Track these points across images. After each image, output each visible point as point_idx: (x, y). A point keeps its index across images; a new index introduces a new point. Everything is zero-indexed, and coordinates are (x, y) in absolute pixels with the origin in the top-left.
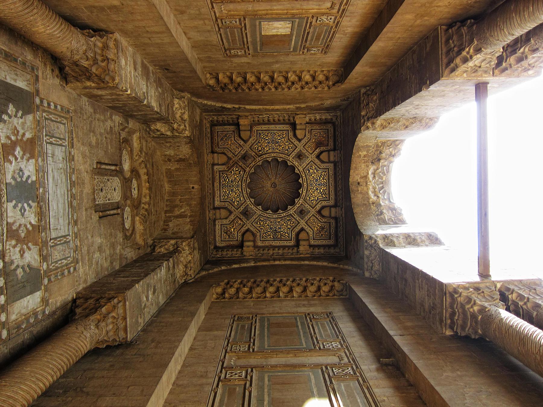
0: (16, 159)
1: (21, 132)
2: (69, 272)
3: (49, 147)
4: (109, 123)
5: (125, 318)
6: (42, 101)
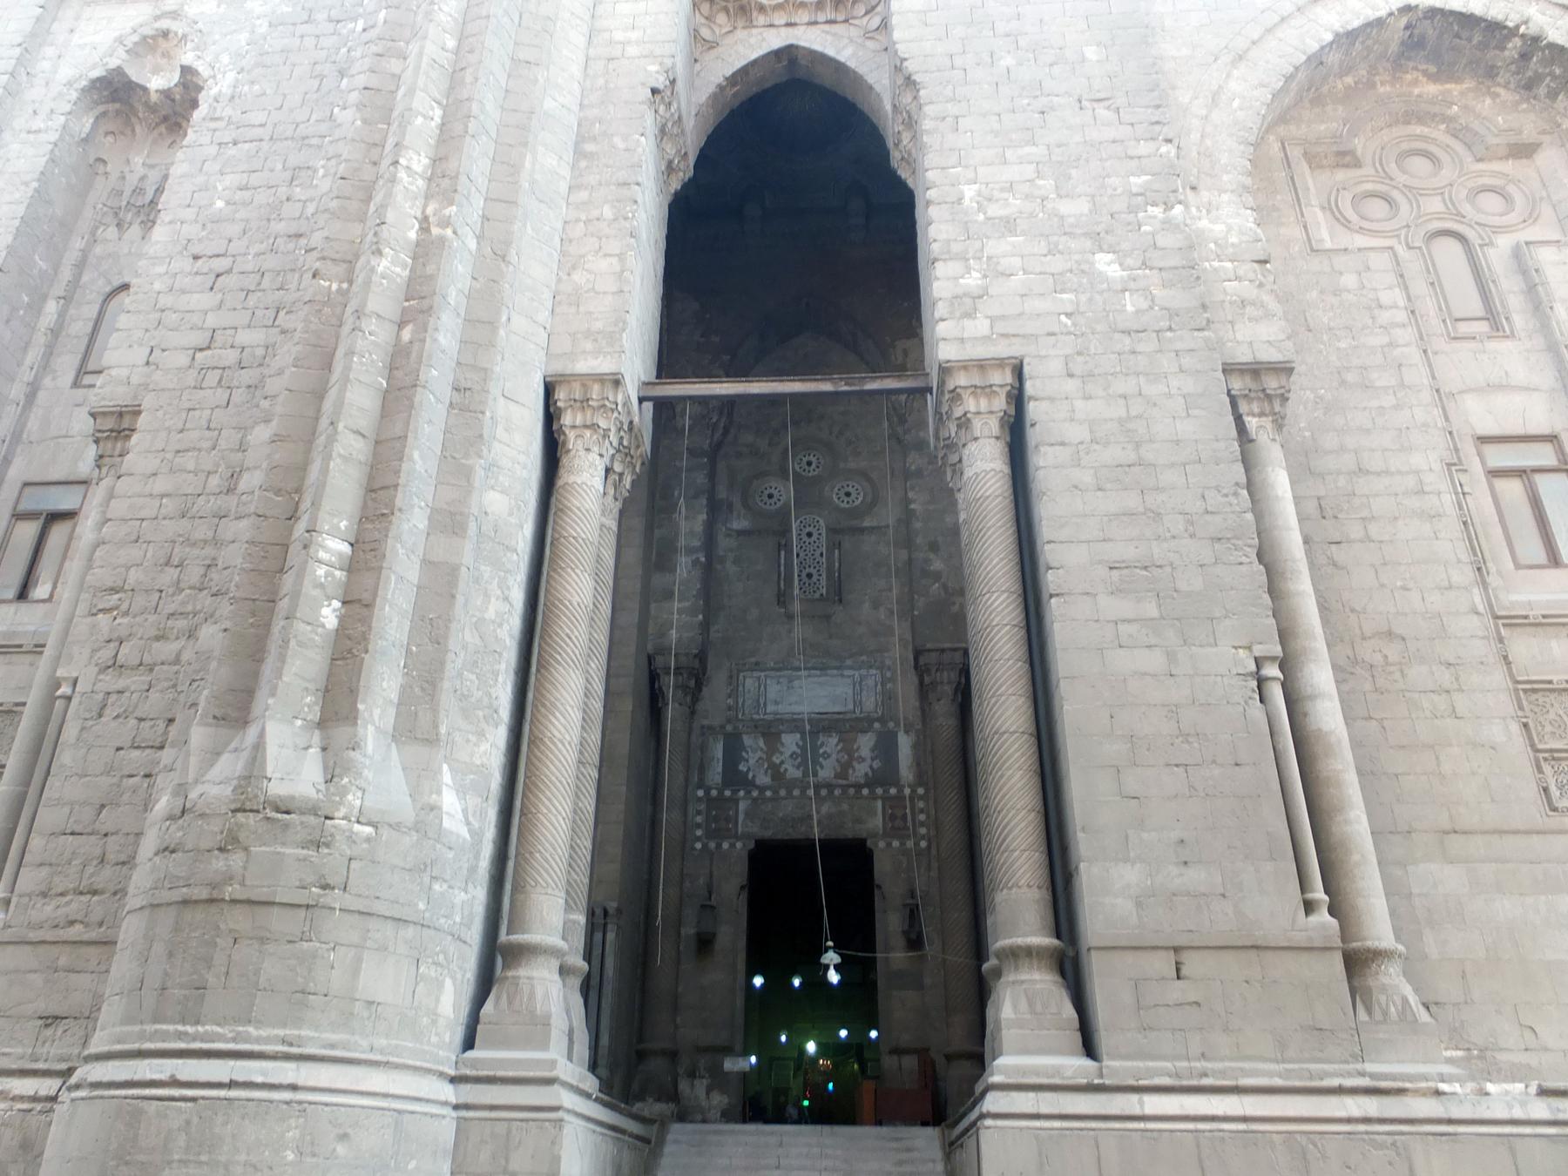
0: (782, 762)
1: (759, 754)
2: (890, 680)
3: (770, 708)
4: (731, 568)
5: (943, 651)
6: (729, 721)
